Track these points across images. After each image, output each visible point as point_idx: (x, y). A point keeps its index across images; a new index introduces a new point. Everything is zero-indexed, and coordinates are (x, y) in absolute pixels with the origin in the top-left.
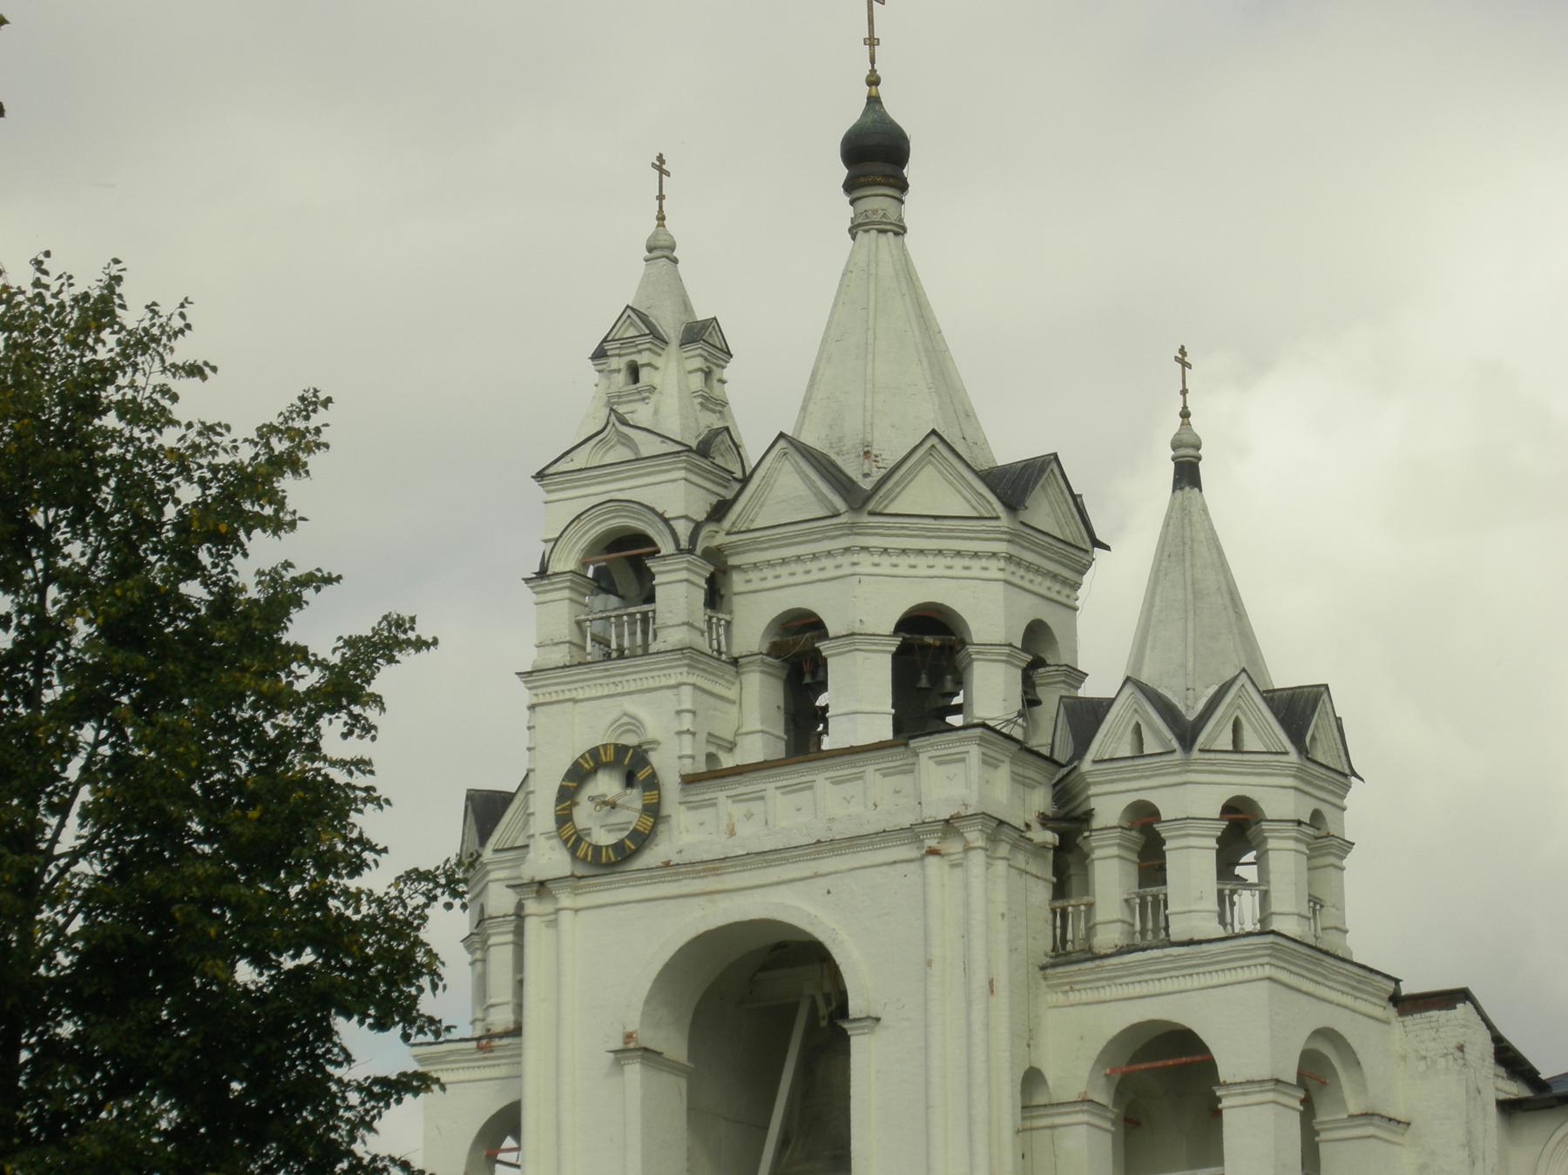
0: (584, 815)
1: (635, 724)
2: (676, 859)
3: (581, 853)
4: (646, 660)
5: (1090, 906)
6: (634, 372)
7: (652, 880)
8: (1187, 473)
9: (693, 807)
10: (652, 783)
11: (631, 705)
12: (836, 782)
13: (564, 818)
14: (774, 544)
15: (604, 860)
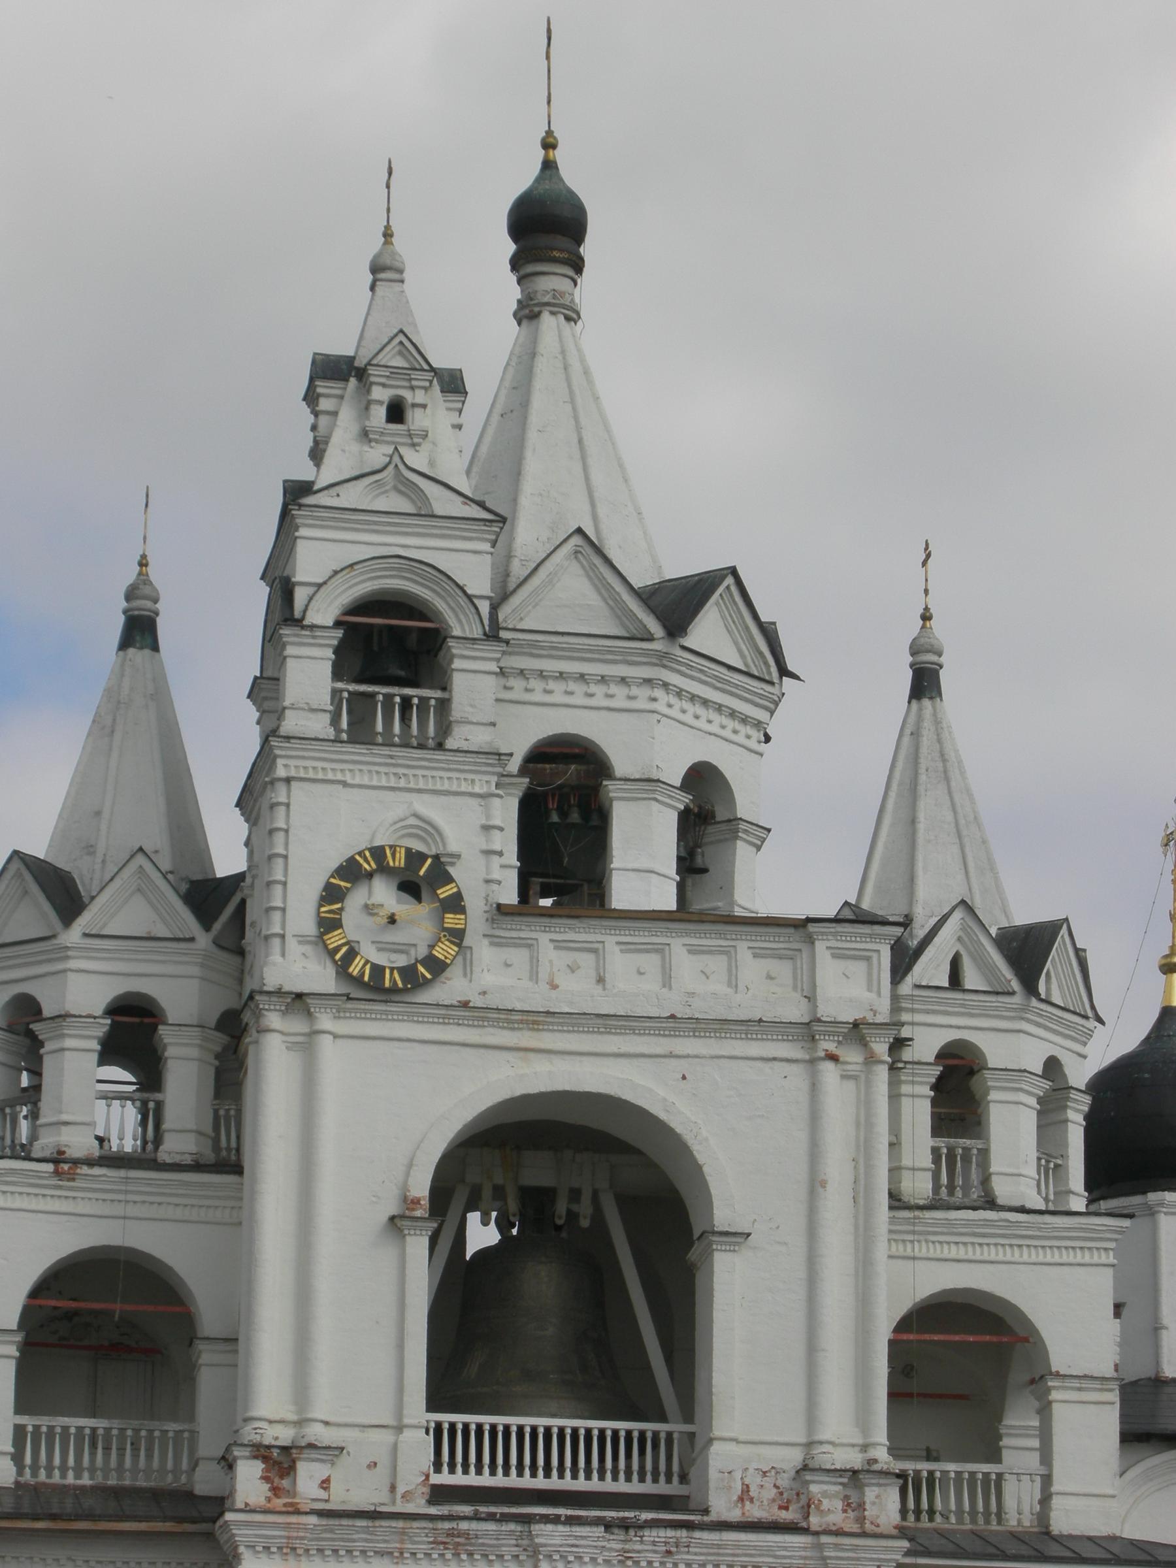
0: (355, 923)
1: (430, 829)
2: (477, 1001)
3: (354, 969)
4: (439, 755)
5: (984, 1153)
6: (396, 412)
7: (445, 1021)
8: (925, 683)
9: (497, 942)
10: (456, 904)
11: (426, 806)
12: (693, 951)
13: (329, 925)
14: (555, 653)
15: (387, 984)
